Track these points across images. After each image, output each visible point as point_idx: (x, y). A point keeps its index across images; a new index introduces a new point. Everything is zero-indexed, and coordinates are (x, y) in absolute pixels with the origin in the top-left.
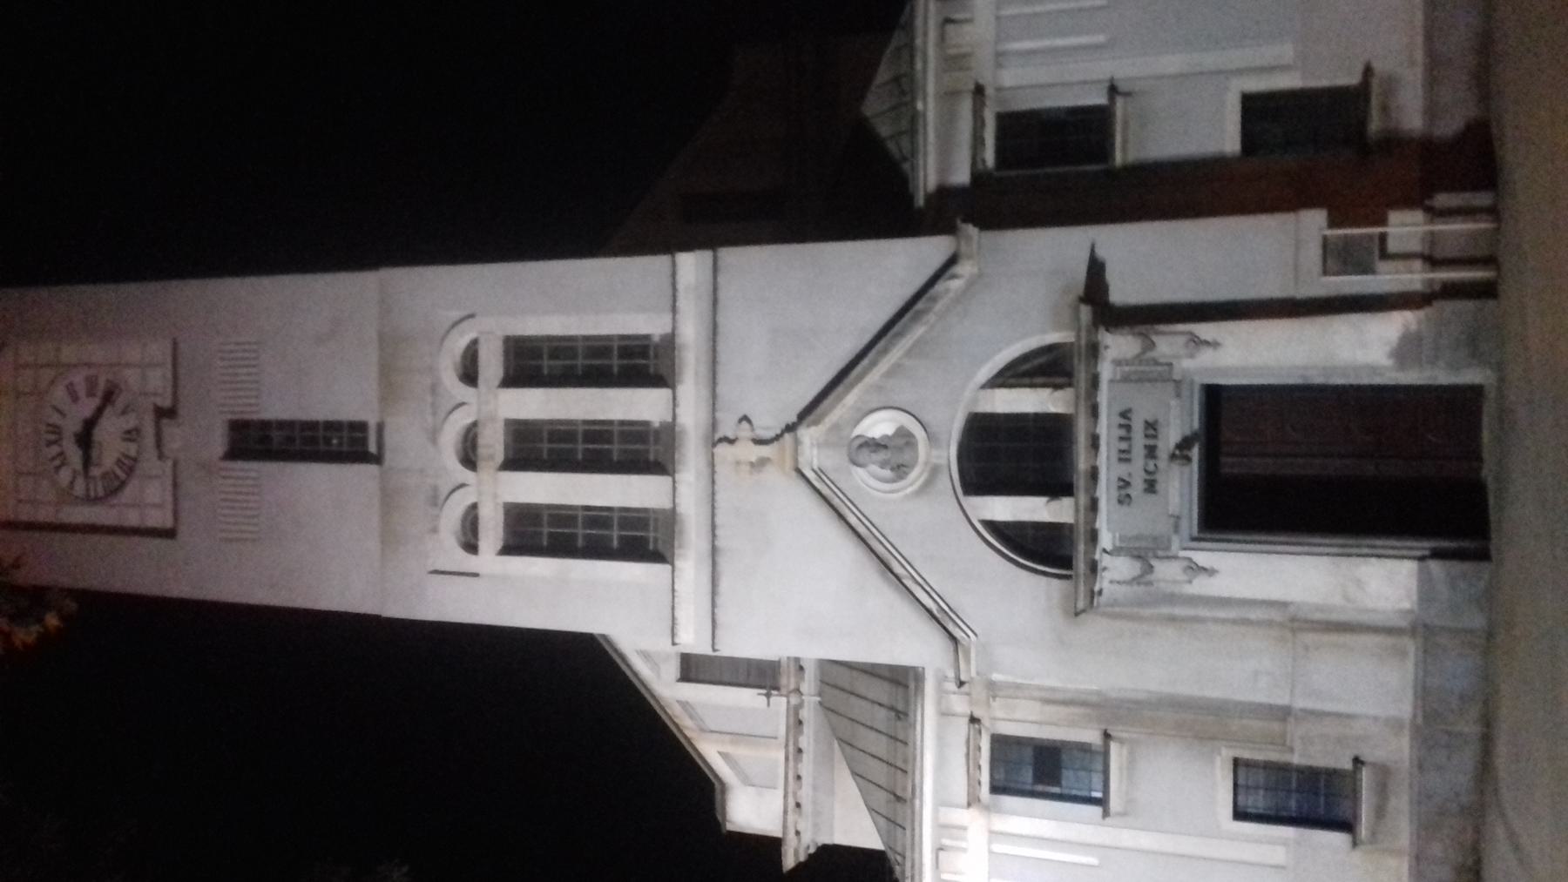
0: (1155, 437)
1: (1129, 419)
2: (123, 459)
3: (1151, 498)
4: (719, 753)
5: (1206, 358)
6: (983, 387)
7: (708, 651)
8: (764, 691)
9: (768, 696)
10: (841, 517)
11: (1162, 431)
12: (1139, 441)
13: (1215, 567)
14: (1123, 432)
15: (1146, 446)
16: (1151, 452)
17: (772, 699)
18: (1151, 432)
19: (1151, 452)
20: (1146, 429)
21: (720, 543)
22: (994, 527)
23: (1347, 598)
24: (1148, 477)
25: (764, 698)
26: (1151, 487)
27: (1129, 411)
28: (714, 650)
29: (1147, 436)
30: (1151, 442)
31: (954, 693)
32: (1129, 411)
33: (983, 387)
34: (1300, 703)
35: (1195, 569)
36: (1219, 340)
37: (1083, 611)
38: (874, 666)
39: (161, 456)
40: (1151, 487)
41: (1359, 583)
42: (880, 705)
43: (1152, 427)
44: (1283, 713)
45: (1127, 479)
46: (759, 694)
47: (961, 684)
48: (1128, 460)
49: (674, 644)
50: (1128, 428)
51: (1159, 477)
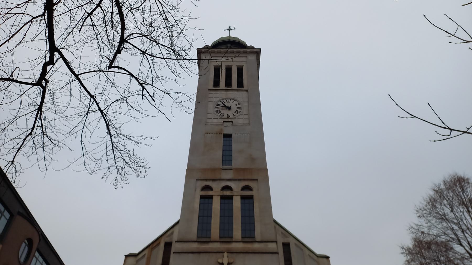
2: (223, 114)
4: (145, 255)
7: (173, 249)
21: (201, 255)
28: (174, 253)
39: (224, 122)
49: (176, 241)
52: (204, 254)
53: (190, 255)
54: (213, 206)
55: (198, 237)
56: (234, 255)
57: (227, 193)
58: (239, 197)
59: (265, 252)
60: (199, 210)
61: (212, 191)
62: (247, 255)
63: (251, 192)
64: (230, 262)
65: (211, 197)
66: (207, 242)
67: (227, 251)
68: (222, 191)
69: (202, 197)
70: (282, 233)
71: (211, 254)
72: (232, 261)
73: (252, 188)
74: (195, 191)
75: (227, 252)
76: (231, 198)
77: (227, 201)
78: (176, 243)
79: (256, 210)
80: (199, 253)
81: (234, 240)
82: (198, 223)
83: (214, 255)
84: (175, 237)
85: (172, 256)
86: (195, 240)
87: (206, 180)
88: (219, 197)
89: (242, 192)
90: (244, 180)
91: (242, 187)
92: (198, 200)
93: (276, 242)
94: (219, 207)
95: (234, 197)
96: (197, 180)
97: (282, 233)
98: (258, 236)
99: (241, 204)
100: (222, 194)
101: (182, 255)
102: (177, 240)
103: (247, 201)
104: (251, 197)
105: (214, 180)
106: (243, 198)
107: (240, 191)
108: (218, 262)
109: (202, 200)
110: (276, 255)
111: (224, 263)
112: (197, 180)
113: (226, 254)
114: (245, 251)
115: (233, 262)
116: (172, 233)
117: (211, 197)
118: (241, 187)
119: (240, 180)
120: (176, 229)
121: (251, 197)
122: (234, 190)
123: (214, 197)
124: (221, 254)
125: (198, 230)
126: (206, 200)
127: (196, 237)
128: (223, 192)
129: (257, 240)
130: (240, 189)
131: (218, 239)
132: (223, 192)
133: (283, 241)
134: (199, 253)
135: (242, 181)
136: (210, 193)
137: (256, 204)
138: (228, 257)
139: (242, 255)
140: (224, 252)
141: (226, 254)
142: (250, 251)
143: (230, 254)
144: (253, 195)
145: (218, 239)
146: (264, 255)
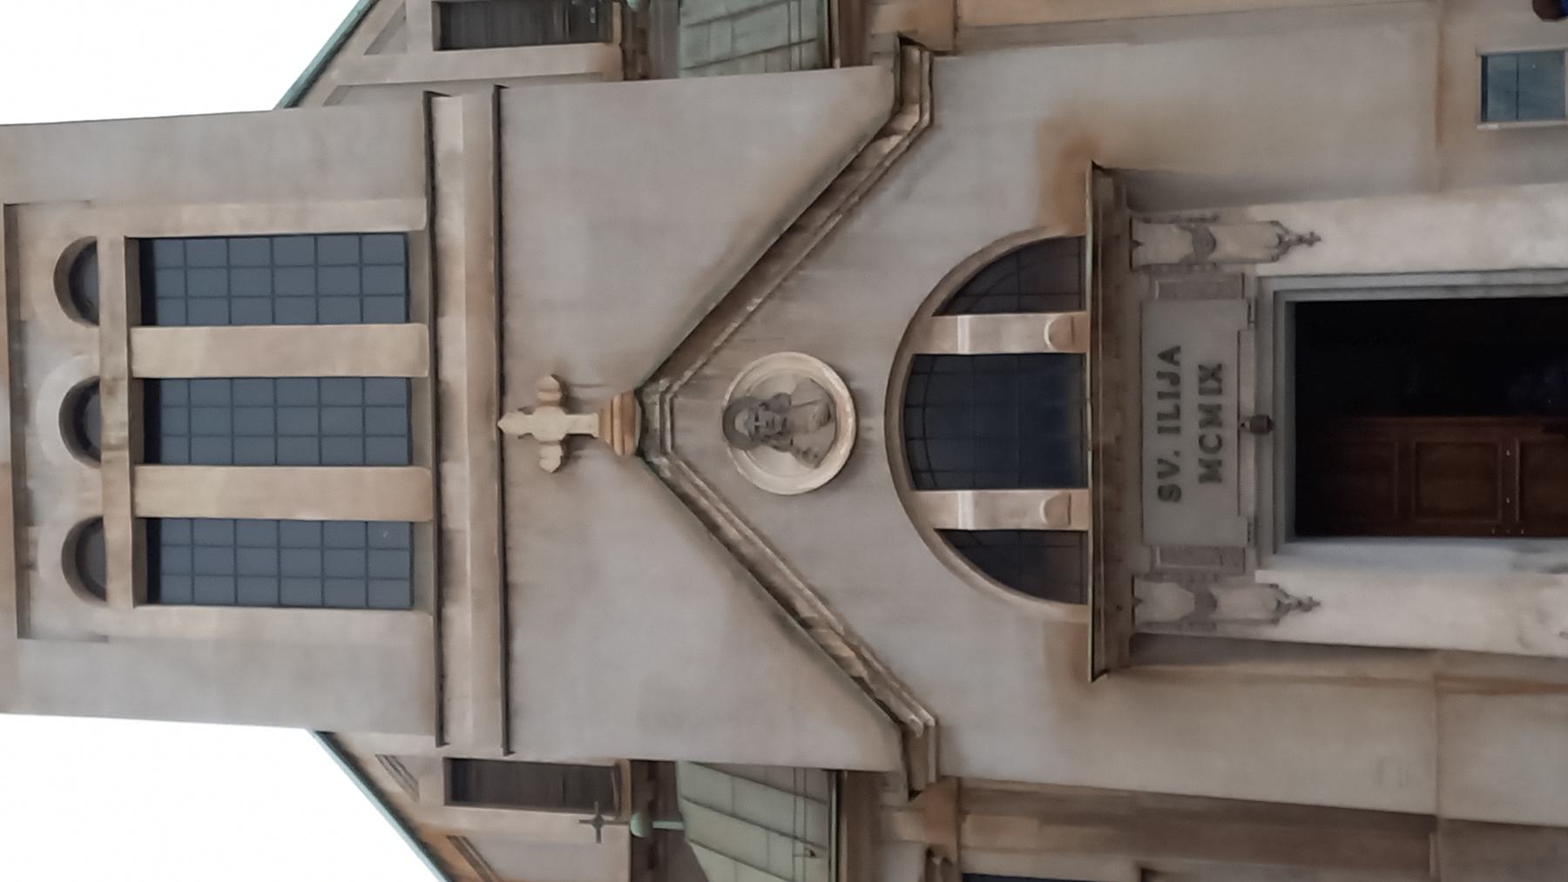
0: (1219, 391)
1: (1177, 364)
3: (1212, 488)
5: (1300, 262)
6: (934, 315)
7: (494, 751)
8: (591, 817)
9: (598, 823)
10: (713, 528)
11: (1230, 379)
12: (1191, 397)
13: (1316, 598)
14: (1164, 386)
15: (1201, 407)
16: (1211, 416)
17: (604, 829)
18: (1212, 384)
19: (1211, 416)
20: (1202, 380)
22: (959, 541)
23: (1521, 640)
24: (1207, 457)
25: (591, 829)
26: (1211, 473)
27: (1178, 349)
28: (508, 751)
29: (1202, 392)
30: (1211, 400)
31: (900, 809)
32: (1178, 349)
33: (934, 315)
34: (1456, 809)
35: (1284, 606)
36: (1318, 232)
37: (1106, 671)
38: (767, 768)
40: (1211, 473)
41: (1543, 617)
42: (782, 834)
43: (1211, 374)
44: (1423, 825)
45: (1174, 460)
46: (583, 822)
47: (913, 793)
48: (1177, 430)
49: (441, 742)
50: (1175, 379)
51: (1228, 456)
52: (516, 558)
53: (520, 645)
54: (211, 511)
55: (412, 604)
56: (515, 369)
57: (115, 417)
58: (143, 335)
59: (491, 173)
60: (236, 603)
61: (106, 522)
62: (511, 287)
63: (102, 249)
64: (558, 396)
65: (150, 531)
66: (442, 537)
67: (495, 409)
68: (105, 455)
69: (150, 591)
70: (373, 49)
71: (515, 517)
72: (553, 383)
73: (73, 245)
74: (104, 639)
75: (501, 414)
76: (149, 394)
77: (172, 421)
78: (447, 739)
79: (230, 219)
80: (506, 588)
81: (426, 373)
82: (323, 606)
83: (516, 496)
84: (418, 745)
85: (526, 752)
86: (431, 619)
87: (24, 567)
88: (148, 472)
89: (104, 316)
90: (14, 298)
91: (70, 316)
92: (167, 619)
93: (429, 97)
94: (218, 475)
95: (145, 369)
96: (24, 630)
97: (373, 49)
98: (406, 215)
99: (187, 323)
100: (126, 454)
101: (518, 697)
102: (432, 739)
103: (166, 283)
104: (143, 252)
105: (23, 514)
106: (146, 312)
107: (94, 330)
108: (557, 470)
109: (168, 585)
110: (506, 98)
111: (561, 437)
112: (24, 630)
113: (513, 424)
114: (493, 299)
115: (555, 376)
116: (393, 762)
117: (150, 531)
118: (70, 321)
119: (17, 330)
120: (365, 743)
121: (143, 252)
122: (95, 372)
123: (146, 510)
124: (512, 452)
125: (367, 606)
126: (171, 559)
127: (411, 617)
128: (111, 448)
129: (422, 223)
130: (81, 329)
131: (421, 475)
132: (111, 448)
133: (430, 45)
134: (506, 588)
135: (23, 317)
136: (119, 537)
137: (191, 220)
138: (527, 411)
139: (514, 322)
140: (501, 432)
141: (513, 424)
142: (491, 266)
143: (510, 400)
144: (123, 239)
145: (421, 475)
146: (510, 173)
